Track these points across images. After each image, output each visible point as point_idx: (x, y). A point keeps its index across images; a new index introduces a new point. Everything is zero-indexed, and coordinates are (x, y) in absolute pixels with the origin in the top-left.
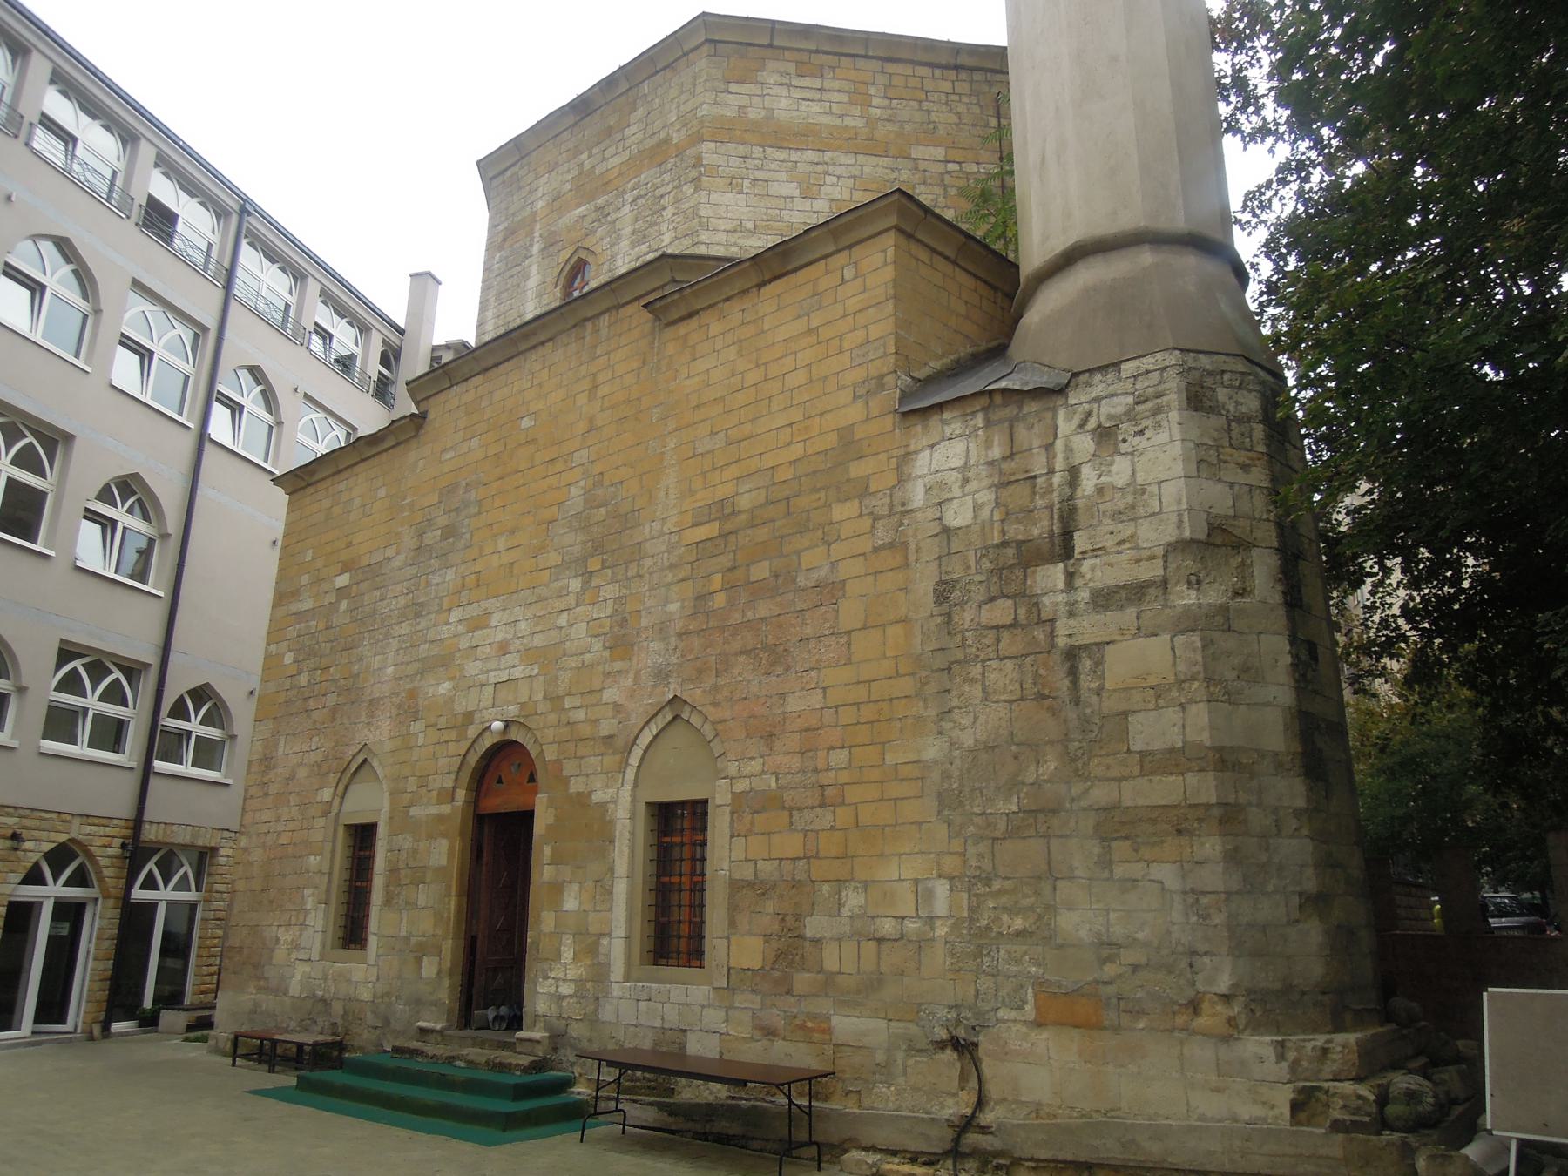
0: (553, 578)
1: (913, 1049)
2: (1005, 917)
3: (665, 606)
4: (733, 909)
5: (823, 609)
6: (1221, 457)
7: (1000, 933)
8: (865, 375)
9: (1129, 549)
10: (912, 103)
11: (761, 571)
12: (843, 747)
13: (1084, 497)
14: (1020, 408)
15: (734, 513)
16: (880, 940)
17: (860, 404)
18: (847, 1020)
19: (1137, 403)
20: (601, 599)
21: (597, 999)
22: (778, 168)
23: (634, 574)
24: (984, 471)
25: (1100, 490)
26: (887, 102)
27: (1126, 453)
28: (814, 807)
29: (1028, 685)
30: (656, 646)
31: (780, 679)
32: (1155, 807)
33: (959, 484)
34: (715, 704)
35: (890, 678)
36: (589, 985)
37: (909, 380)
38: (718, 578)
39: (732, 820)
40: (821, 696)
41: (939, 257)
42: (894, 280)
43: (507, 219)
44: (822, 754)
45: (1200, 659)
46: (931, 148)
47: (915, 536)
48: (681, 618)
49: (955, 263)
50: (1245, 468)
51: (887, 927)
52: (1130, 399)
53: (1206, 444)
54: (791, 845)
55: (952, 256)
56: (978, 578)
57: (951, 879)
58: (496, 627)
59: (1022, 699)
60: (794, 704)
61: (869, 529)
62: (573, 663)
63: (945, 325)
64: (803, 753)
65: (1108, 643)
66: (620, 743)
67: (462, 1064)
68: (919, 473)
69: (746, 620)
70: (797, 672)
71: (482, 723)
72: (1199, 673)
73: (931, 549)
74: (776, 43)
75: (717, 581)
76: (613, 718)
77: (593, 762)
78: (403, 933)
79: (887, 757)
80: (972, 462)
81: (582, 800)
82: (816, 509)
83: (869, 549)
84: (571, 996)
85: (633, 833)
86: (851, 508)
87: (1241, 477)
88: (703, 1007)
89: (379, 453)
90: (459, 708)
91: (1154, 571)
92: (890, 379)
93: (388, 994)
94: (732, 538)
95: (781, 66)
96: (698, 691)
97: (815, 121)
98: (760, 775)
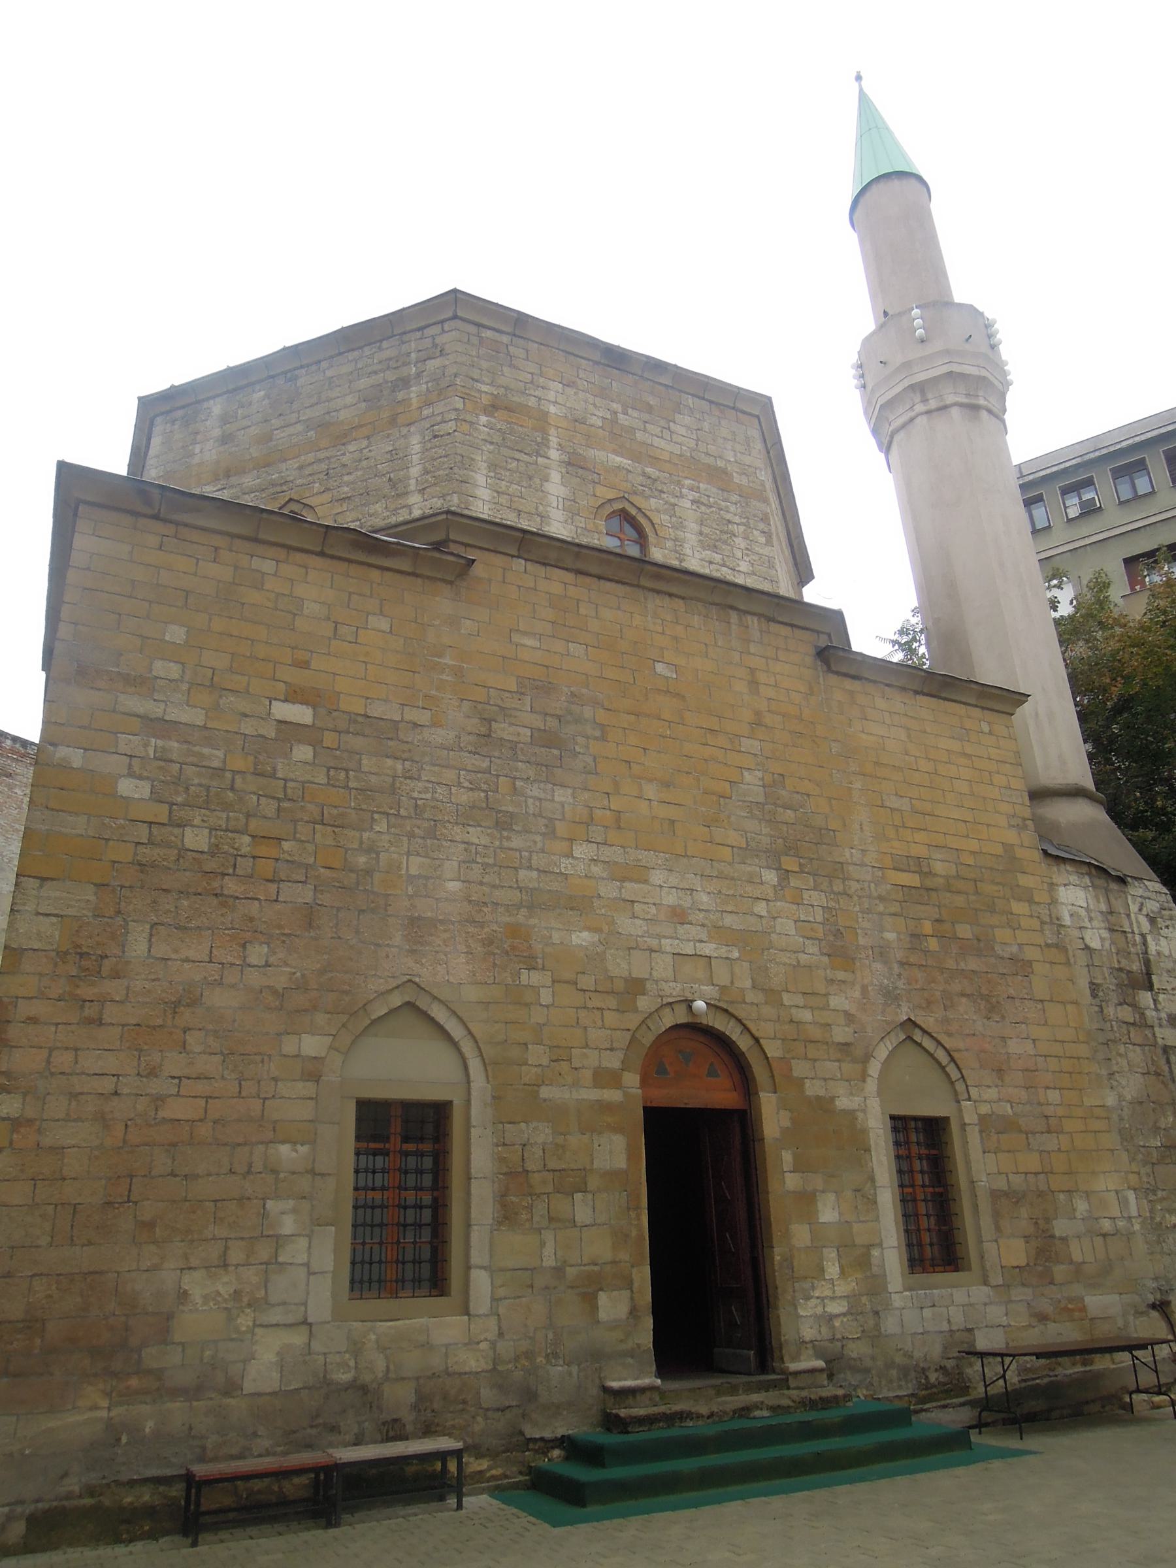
1: (1139, 1313)
2: (1167, 1215)
4: (996, 1215)
7: (1167, 1227)
16: (1104, 1235)
18: (1094, 1298)
21: (877, 1313)
28: (1042, 1133)
29: (1150, 1066)
34: (950, 1035)
36: (864, 1299)
51: (1107, 1225)
54: (1032, 1162)
57: (1135, 1190)
59: (1148, 1073)
67: (766, 1413)
71: (662, 997)
75: (928, 927)
76: (848, 1025)
77: (831, 1067)
78: (549, 1261)
81: (824, 1105)
84: (844, 1315)
88: (985, 1304)
90: (619, 966)
93: (529, 1355)
96: (932, 1019)
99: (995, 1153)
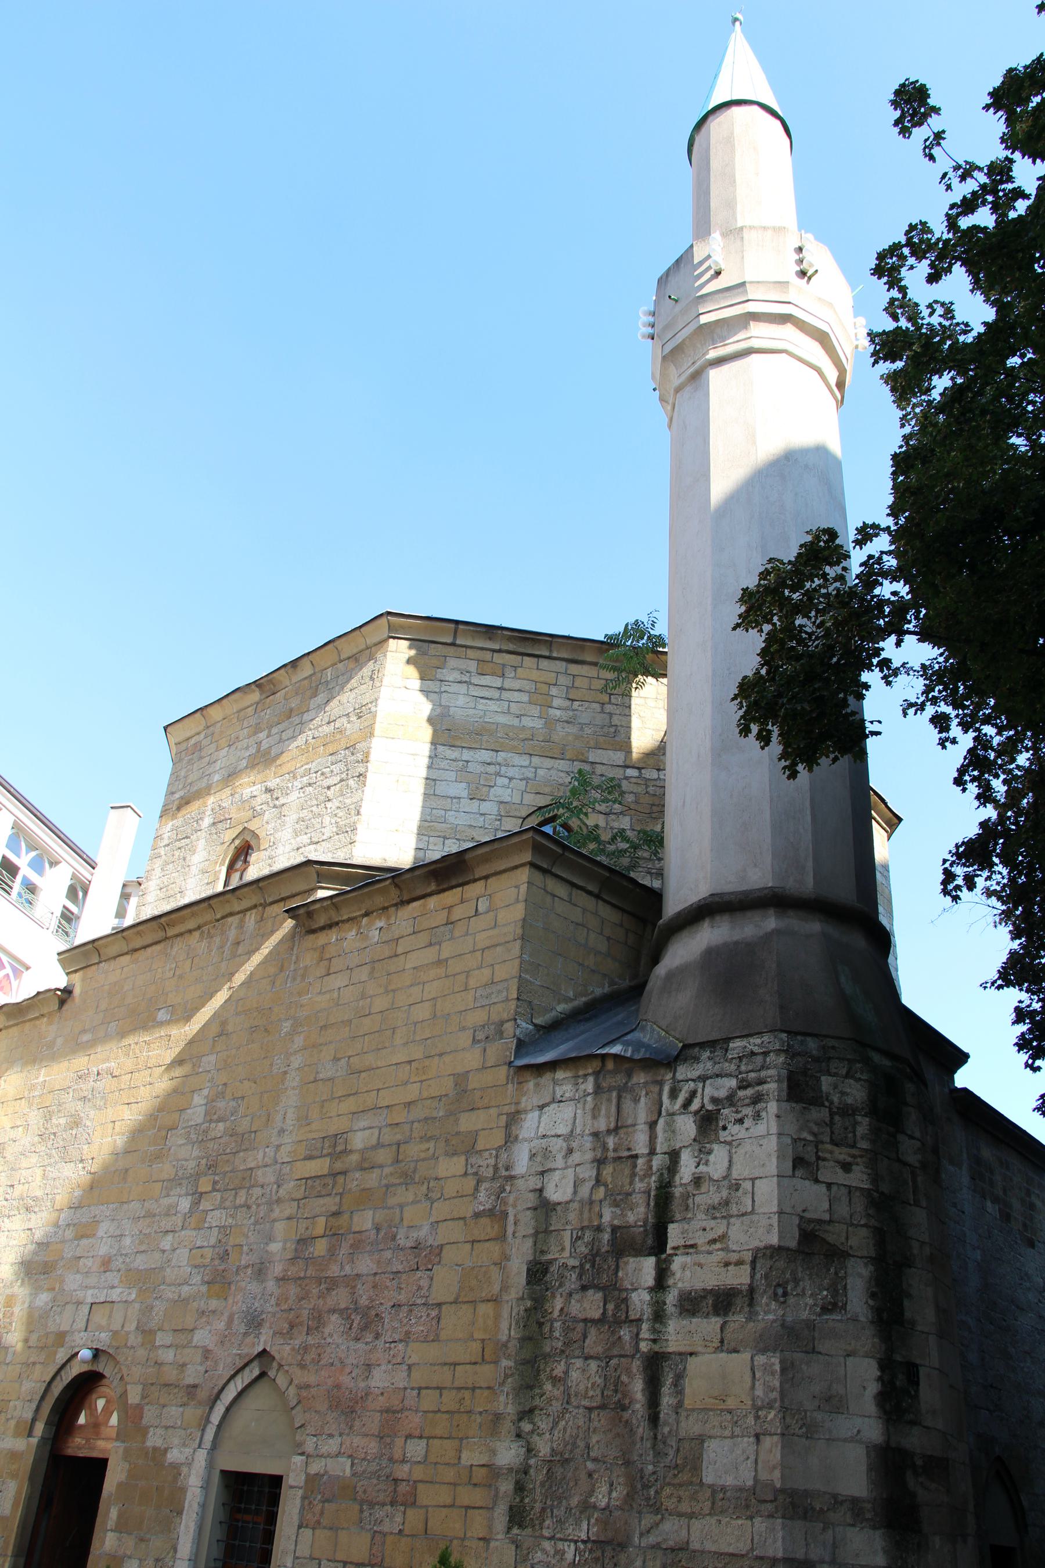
0: (164, 1192)
3: (267, 1244)
5: (419, 1274)
6: (820, 1154)
8: (486, 1018)
9: (718, 1250)
10: (595, 705)
11: (365, 1221)
12: (421, 1437)
13: (681, 1185)
14: (629, 1076)
15: (345, 1152)
17: (477, 1050)
19: (740, 1088)
20: (206, 1225)
22: (447, 767)
23: (242, 1202)
24: (588, 1142)
25: (697, 1181)
26: (568, 703)
27: (725, 1142)
28: (383, 1505)
30: (254, 1287)
31: (369, 1347)
32: (722, 1554)
33: (563, 1153)
34: (302, 1366)
35: (475, 1363)
37: (531, 1027)
38: (322, 1220)
39: (302, 1508)
40: (405, 1374)
41: (579, 892)
42: (524, 920)
43: (184, 787)
44: (399, 1442)
45: (777, 1384)
46: (610, 752)
47: (514, 1206)
48: (280, 1261)
49: (598, 897)
50: (846, 1167)
52: (733, 1083)
53: (805, 1139)
55: (596, 891)
56: (572, 1262)
58: (102, 1237)
59: (602, 1407)
60: (379, 1379)
61: (471, 1192)
62: (170, 1293)
63: (580, 964)
64: (382, 1438)
65: (691, 1354)
66: (203, 1394)
68: (526, 1136)
69: (343, 1274)
70: (386, 1342)
71: (73, 1347)
72: (775, 1400)
73: (527, 1224)
74: (458, 642)
79: (464, 1456)
80: (578, 1131)
82: (423, 1160)
83: (469, 1214)
85: (203, 1506)
86: (457, 1165)
87: (840, 1176)
89: (25, 1022)
91: (739, 1278)
92: (509, 1027)
94: (340, 1179)
95: (462, 664)
96: (288, 1348)
97: (490, 720)
98: (337, 1456)
99: (314, 1529)
